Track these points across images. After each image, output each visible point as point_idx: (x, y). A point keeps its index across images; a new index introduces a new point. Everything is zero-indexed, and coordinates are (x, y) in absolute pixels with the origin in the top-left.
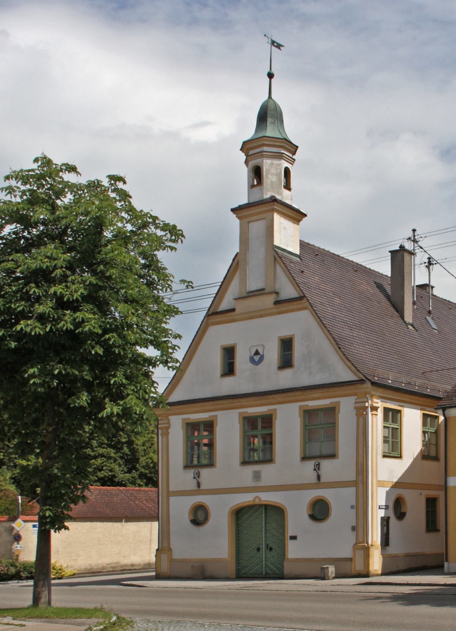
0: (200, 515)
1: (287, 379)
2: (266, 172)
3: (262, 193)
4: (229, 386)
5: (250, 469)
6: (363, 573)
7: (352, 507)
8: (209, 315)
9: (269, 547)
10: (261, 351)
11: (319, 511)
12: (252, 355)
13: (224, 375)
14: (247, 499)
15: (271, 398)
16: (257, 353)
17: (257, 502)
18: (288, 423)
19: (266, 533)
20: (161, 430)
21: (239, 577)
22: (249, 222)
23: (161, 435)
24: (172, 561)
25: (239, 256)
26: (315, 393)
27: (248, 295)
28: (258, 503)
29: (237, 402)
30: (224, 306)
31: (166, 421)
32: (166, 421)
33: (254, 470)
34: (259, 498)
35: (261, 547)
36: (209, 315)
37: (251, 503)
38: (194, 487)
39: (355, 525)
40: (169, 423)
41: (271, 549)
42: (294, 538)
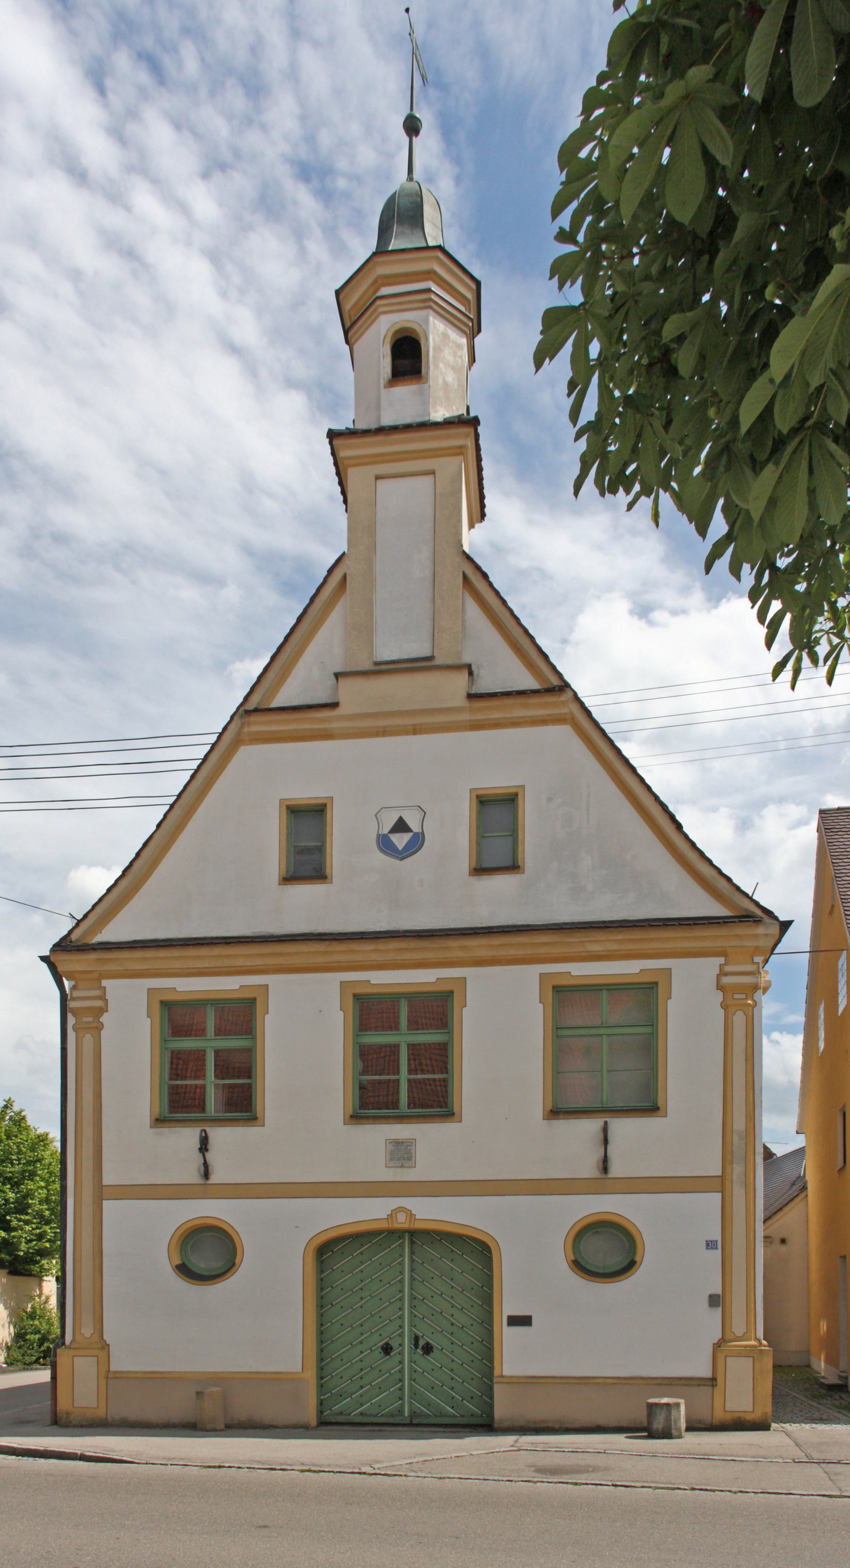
0: (207, 1255)
1: (497, 900)
2: (434, 348)
3: (425, 404)
4: (305, 908)
5: (379, 1135)
6: (749, 1417)
7: (710, 1245)
8: (248, 712)
9: (422, 1343)
10: (413, 823)
11: (606, 1252)
12: (386, 830)
13: (289, 878)
14: (372, 1212)
15: (455, 948)
16: (401, 826)
17: (402, 1221)
18: (305, 1037)
19: (412, 1307)
20: (75, 1014)
21: (330, 1423)
22: (378, 478)
23: (75, 1029)
24: (109, 1377)
25: (346, 561)
26: (597, 943)
27: (373, 668)
28: (406, 1226)
29: (340, 952)
30: (289, 694)
31: (97, 993)
32: (97, 993)
33: (394, 1136)
34: (410, 1215)
35: (394, 1344)
36: (248, 712)
37: (384, 1225)
38: (191, 1175)
39: (718, 1290)
40: (103, 998)
41: (428, 1349)
42: (522, 1321)
